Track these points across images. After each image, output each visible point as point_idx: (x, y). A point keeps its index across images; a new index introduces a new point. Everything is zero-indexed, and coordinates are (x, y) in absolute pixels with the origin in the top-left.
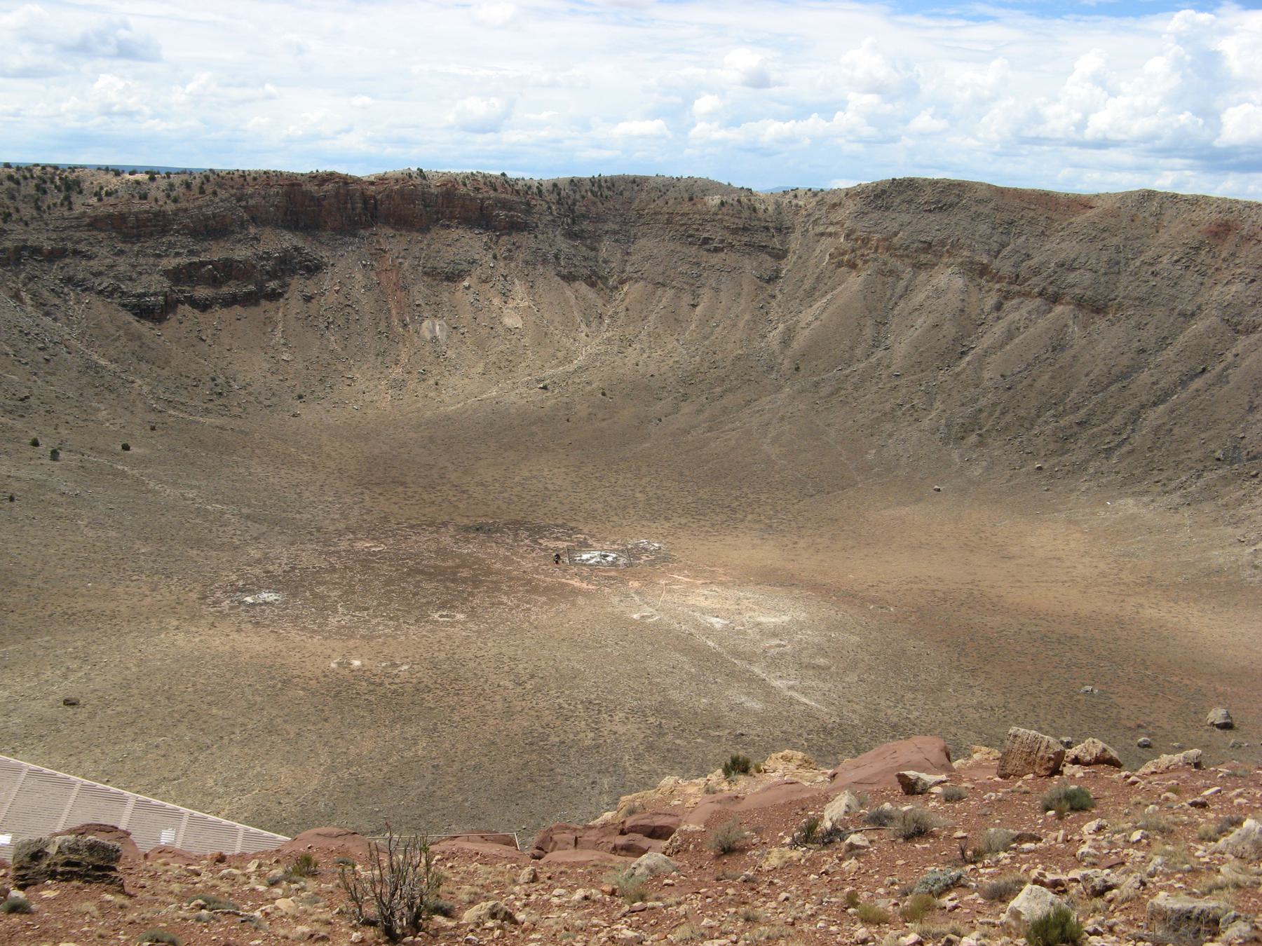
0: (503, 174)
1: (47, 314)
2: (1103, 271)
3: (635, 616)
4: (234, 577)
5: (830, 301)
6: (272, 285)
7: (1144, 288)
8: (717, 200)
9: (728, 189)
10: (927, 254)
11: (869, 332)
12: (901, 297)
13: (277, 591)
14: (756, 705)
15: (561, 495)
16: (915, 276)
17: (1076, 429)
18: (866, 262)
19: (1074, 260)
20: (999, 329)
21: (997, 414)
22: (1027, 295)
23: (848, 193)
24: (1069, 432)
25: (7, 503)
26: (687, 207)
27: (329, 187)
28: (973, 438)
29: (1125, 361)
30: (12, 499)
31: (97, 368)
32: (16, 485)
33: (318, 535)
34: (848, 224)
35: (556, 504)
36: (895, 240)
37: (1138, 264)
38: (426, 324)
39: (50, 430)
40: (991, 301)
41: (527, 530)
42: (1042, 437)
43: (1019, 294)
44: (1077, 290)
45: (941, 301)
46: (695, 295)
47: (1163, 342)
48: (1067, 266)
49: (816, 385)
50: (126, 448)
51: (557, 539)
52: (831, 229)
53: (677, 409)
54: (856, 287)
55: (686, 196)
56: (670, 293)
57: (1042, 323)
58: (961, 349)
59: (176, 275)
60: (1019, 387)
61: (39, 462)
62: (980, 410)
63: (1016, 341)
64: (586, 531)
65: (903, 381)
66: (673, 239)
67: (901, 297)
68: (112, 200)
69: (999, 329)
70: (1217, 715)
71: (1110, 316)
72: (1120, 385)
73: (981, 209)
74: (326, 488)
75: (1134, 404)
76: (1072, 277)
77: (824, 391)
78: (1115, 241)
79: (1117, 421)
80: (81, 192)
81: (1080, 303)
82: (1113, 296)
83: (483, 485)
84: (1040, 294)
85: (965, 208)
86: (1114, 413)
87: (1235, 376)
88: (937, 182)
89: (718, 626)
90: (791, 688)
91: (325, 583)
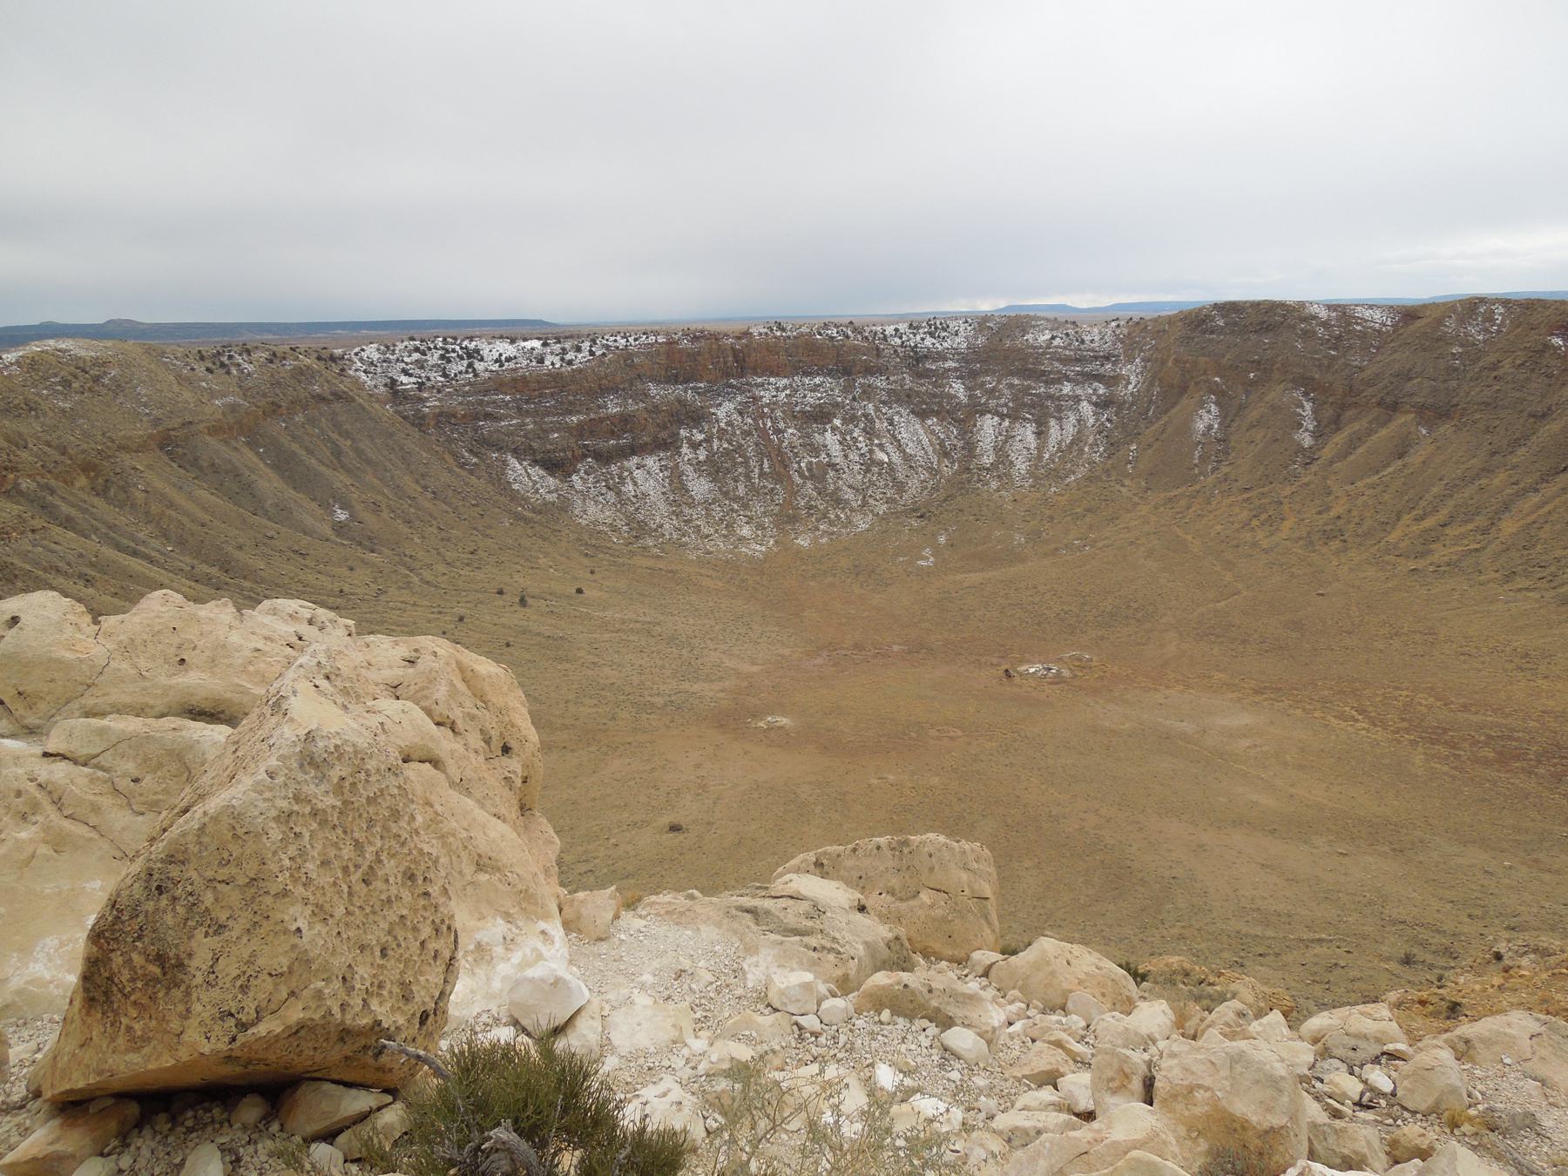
1: (471, 472)
6: (664, 435)
9: (1055, 324)
27: (703, 343)
30: (508, 645)
31: (527, 521)
47: (1516, 443)
50: (579, 591)
57: (1384, 432)
59: (580, 431)
68: (511, 365)
80: (482, 359)
81: (1421, 410)
82: (1455, 401)
84: (1379, 404)
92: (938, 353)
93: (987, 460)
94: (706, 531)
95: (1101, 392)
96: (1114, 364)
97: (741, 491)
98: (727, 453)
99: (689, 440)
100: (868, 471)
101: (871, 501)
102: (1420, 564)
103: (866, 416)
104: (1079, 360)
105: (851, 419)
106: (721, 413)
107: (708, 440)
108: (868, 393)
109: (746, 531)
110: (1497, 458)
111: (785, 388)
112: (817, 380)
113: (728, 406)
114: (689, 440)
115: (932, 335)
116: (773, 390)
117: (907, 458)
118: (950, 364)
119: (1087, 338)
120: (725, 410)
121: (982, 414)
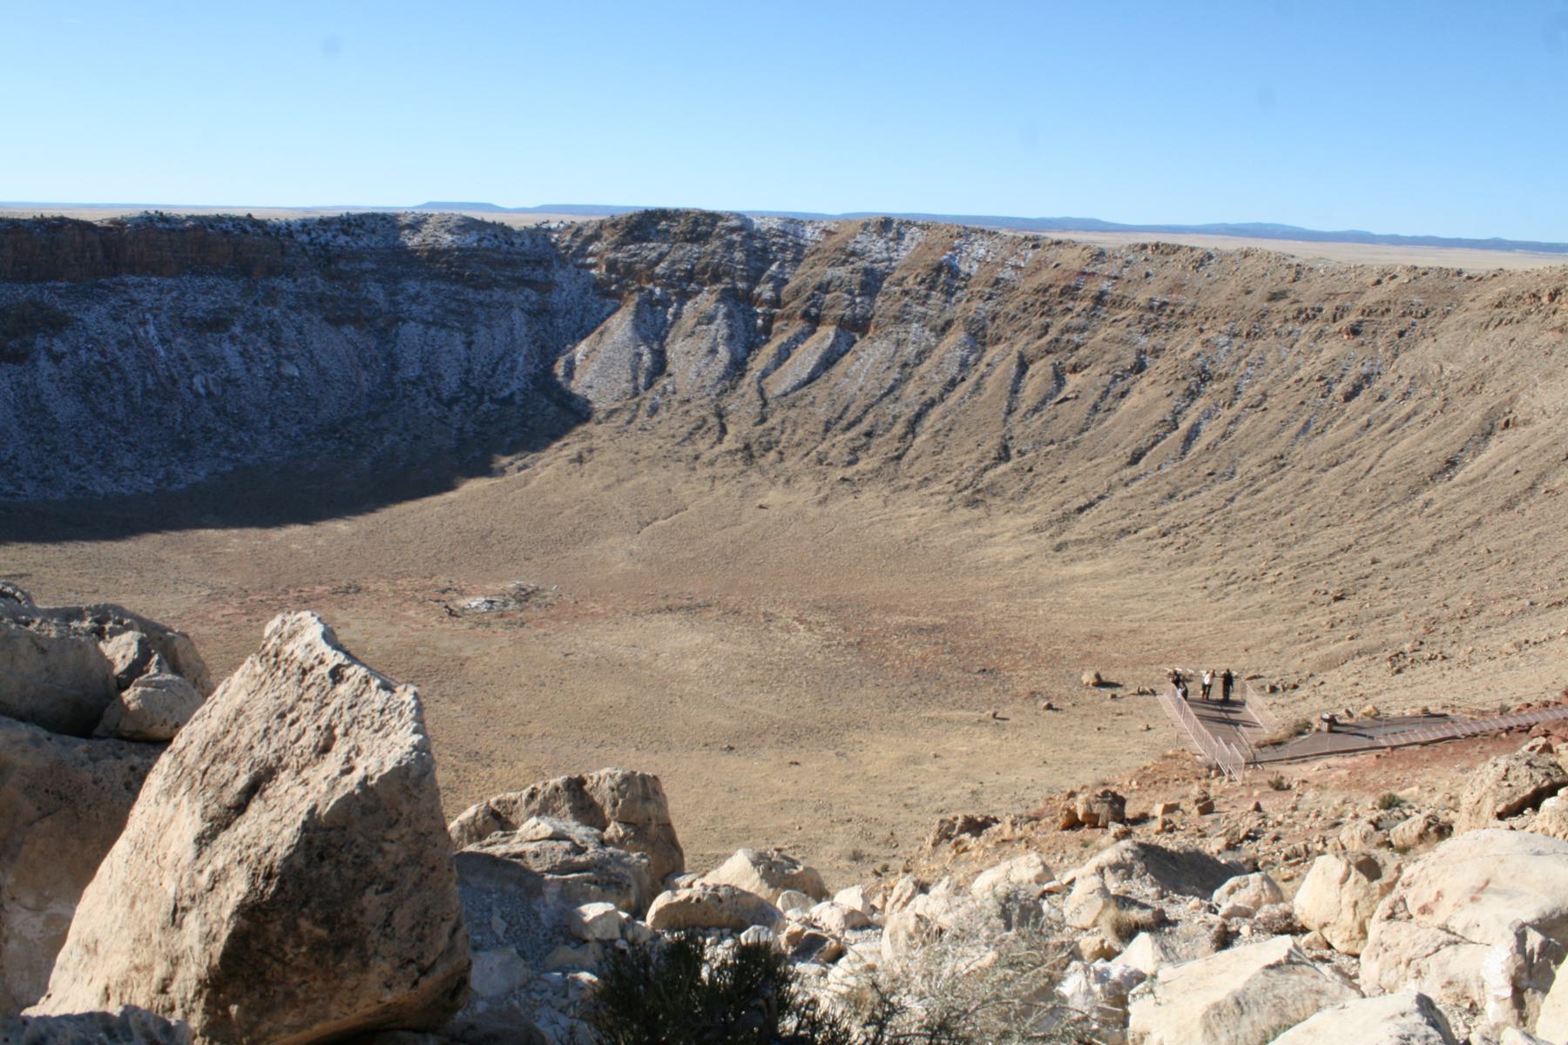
7: (897, 307)
10: (684, 285)
11: (647, 358)
16: (682, 304)
17: (864, 440)
18: (632, 292)
21: (789, 431)
22: (789, 317)
23: (601, 225)
24: (857, 443)
38: (197, 380)
43: (782, 317)
45: (713, 327)
47: (921, 356)
69: (770, 350)
70: (1088, 677)
73: (735, 237)
75: (909, 413)
79: (899, 429)
85: (720, 236)
87: (990, 384)
92: (352, 253)
93: (411, 372)
94: (76, 460)
95: (533, 299)
96: (546, 269)
97: (120, 412)
98: (101, 366)
99: (49, 351)
100: (275, 386)
101: (281, 423)
102: (849, 472)
103: (271, 323)
104: (509, 263)
105: (253, 327)
106: (90, 318)
107: (75, 351)
108: (271, 297)
109: (127, 462)
110: (908, 370)
111: (170, 290)
112: (211, 281)
113: (100, 310)
114: (49, 351)
115: (346, 233)
116: (151, 292)
117: (321, 372)
118: (367, 265)
119: (517, 241)
120: (95, 317)
121: (404, 322)
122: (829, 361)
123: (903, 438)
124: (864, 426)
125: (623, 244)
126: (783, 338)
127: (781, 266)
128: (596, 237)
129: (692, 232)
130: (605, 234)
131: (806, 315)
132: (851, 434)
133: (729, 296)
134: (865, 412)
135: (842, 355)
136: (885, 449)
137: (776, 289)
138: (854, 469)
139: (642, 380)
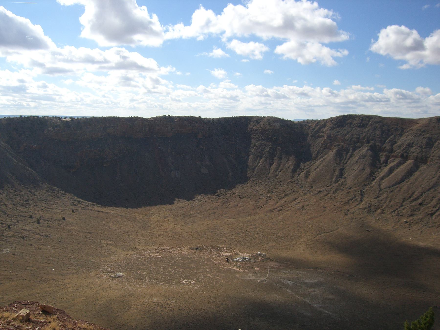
0: (200, 117)
2: (424, 147)
3: (259, 281)
4: (106, 267)
5: (322, 161)
8: (278, 125)
11: (337, 172)
12: (349, 159)
13: (123, 272)
14: (309, 314)
15: (226, 235)
16: (354, 150)
17: (418, 206)
18: (335, 146)
19: (413, 143)
20: (386, 169)
22: (396, 157)
24: (415, 207)
25: (22, 240)
26: (268, 127)
28: (379, 211)
29: (434, 180)
32: (25, 232)
33: (137, 251)
34: (328, 132)
35: (225, 239)
36: (346, 137)
37: (437, 144)
39: (36, 212)
40: (382, 159)
41: (215, 249)
42: (405, 210)
44: (415, 154)
45: (365, 160)
46: (273, 160)
48: (410, 145)
49: (319, 192)
51: (227, 252)
52: (321, 134)
53: (267, 202)
54: (332, 156)
55: (267, 123)
56: (263, 159)
57: (402, 167)
58: (372, 178)
60: (395, 191)
61: (32, 224)
62: (382, 200)
63: (393, 174)
64: (237, 249)
65: (352, 190)
66: (263, 140)
67: (349, 159)
71: (428, 164)
72: (433, 189)
73: (377, 125)
74: (138, 234)
76: (412, 149)
77: (322, 195)
78: (428, 135)
82: (428, 156)
83: (197, 232)
85: (371, 125)
86: (432, 200)
88: (360, 116)
89: (290, 284)
90: (320, 307)
91: (141, 269)
122: (410, 173)
123: (434, 206)
124: (419, 201)
125: (334, 128)
126: (392, 164)
127: (395, 136)
128: (324, 126)
129: (360, 123)
130: (328, 124)
131: (402, 156)
132: (413, 204)
133: (373, 149)
134: (421, 195)
135: (414, 172)
136: (427, 211)
137: (392, 145)
138: (411, 218)
139: (334, 179)
